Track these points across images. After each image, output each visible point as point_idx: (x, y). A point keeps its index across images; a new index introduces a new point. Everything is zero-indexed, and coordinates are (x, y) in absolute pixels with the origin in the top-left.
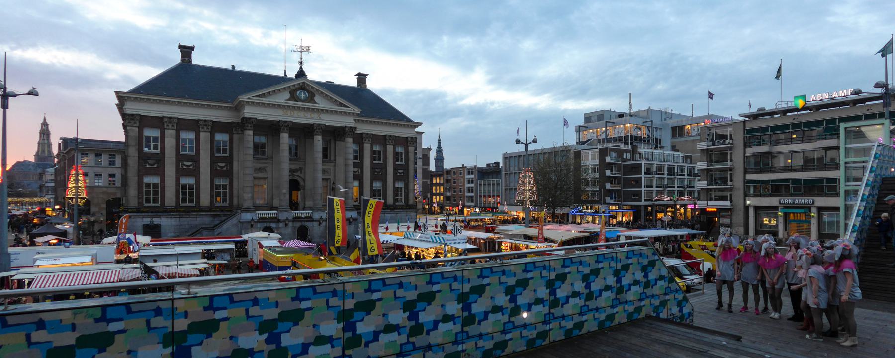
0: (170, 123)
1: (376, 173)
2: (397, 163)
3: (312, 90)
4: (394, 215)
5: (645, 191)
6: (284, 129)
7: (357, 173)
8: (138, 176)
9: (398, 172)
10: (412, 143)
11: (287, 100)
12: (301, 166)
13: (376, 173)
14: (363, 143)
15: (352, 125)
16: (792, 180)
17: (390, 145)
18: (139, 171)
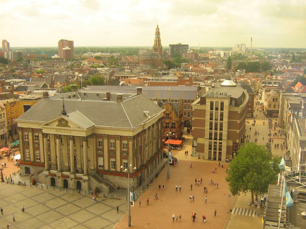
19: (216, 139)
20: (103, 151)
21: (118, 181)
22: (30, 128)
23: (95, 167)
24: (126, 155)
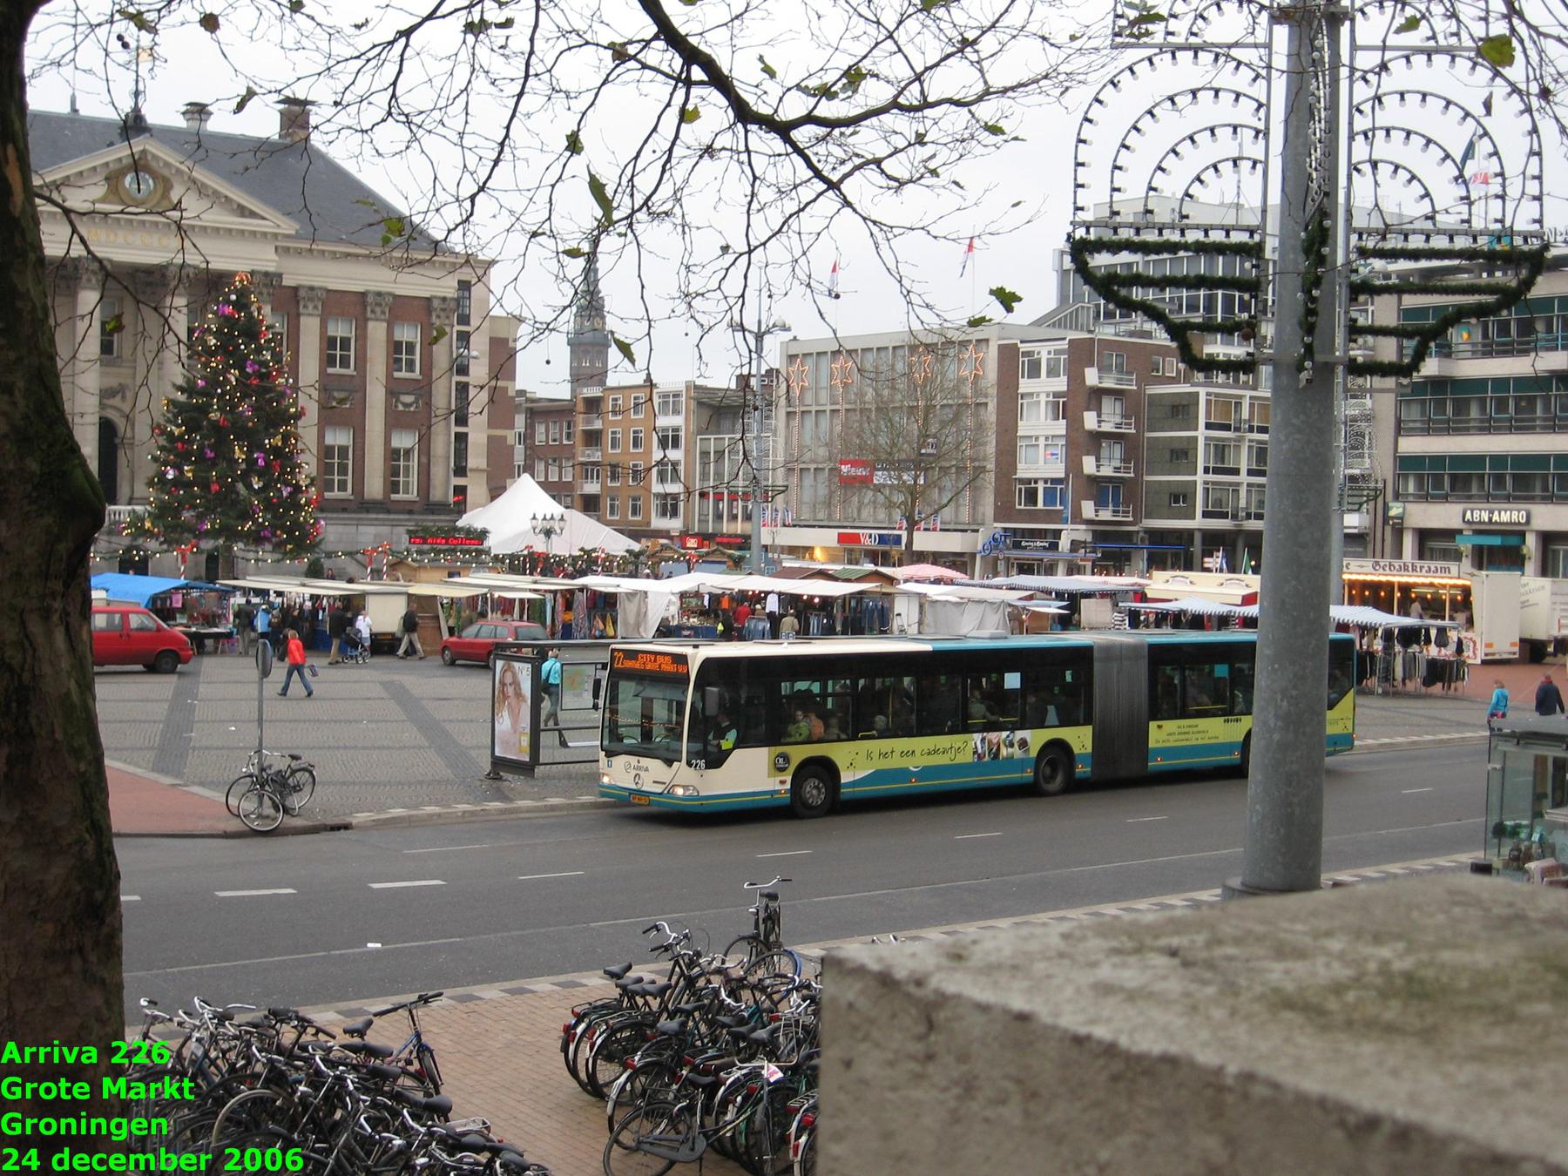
2: (397, 375)
3: (166, 172)
5: (1206, 483)
6: (89, 280)
10: (442, 314)
11: (103, 200)
12: (122, 381)
14: (298, 315)
15: (271, 268)
16: (1513, 456)
17: (377, 320)
24: (416, 401)
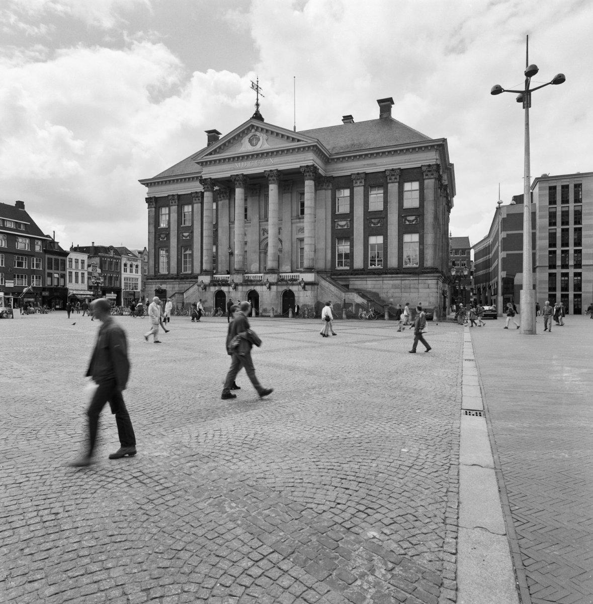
0: (173, 200)
1: (372, 225)
4: (398, 282)
7: (346, 227)
8: (155, 249)
9: (406, 219)
10: (429, 173)
13: (372, 225)
18: (155, 244)
19: (565, 266)
20: (352, 221)
21: (390, 295)
22: (173, 195)
23: (329, 265)
